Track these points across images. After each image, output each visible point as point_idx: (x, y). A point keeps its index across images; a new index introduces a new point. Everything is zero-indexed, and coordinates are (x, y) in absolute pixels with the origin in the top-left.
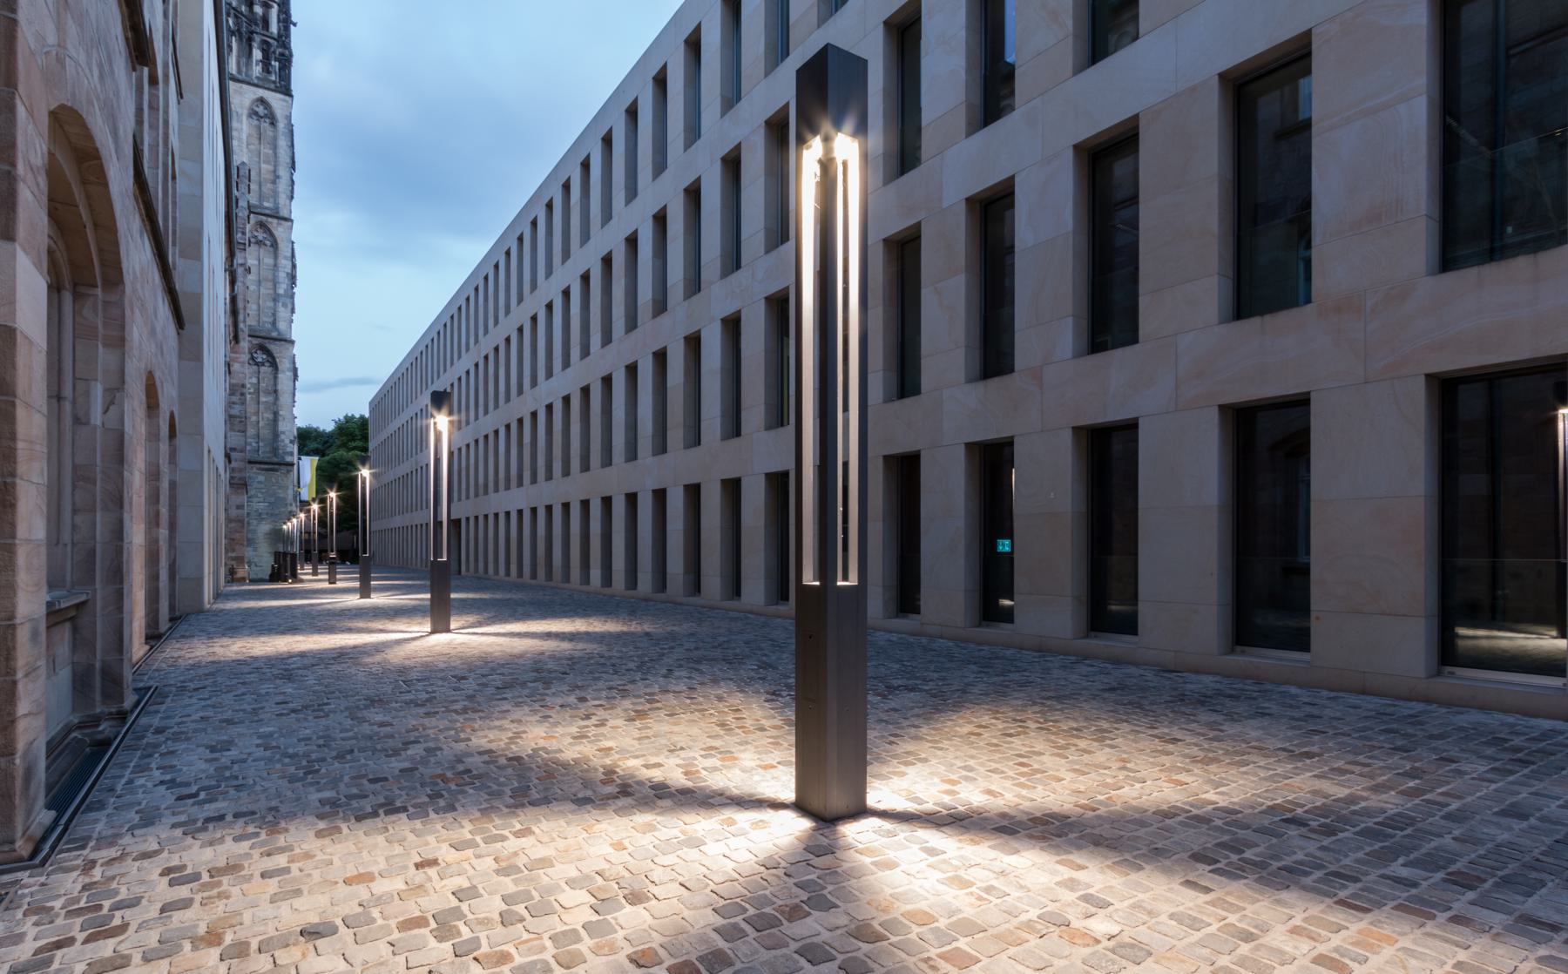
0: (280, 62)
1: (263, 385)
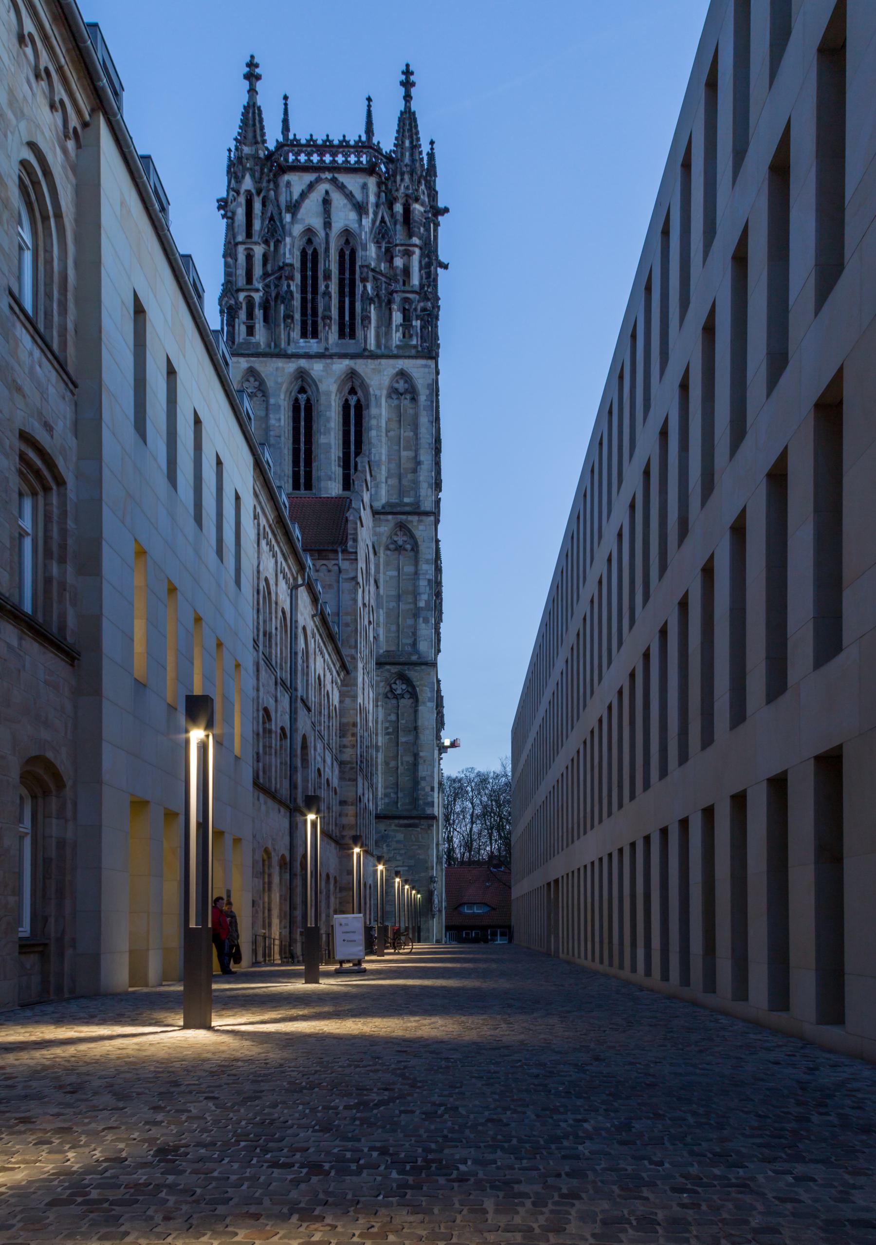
0: (422, 320)
1: (402, 722)
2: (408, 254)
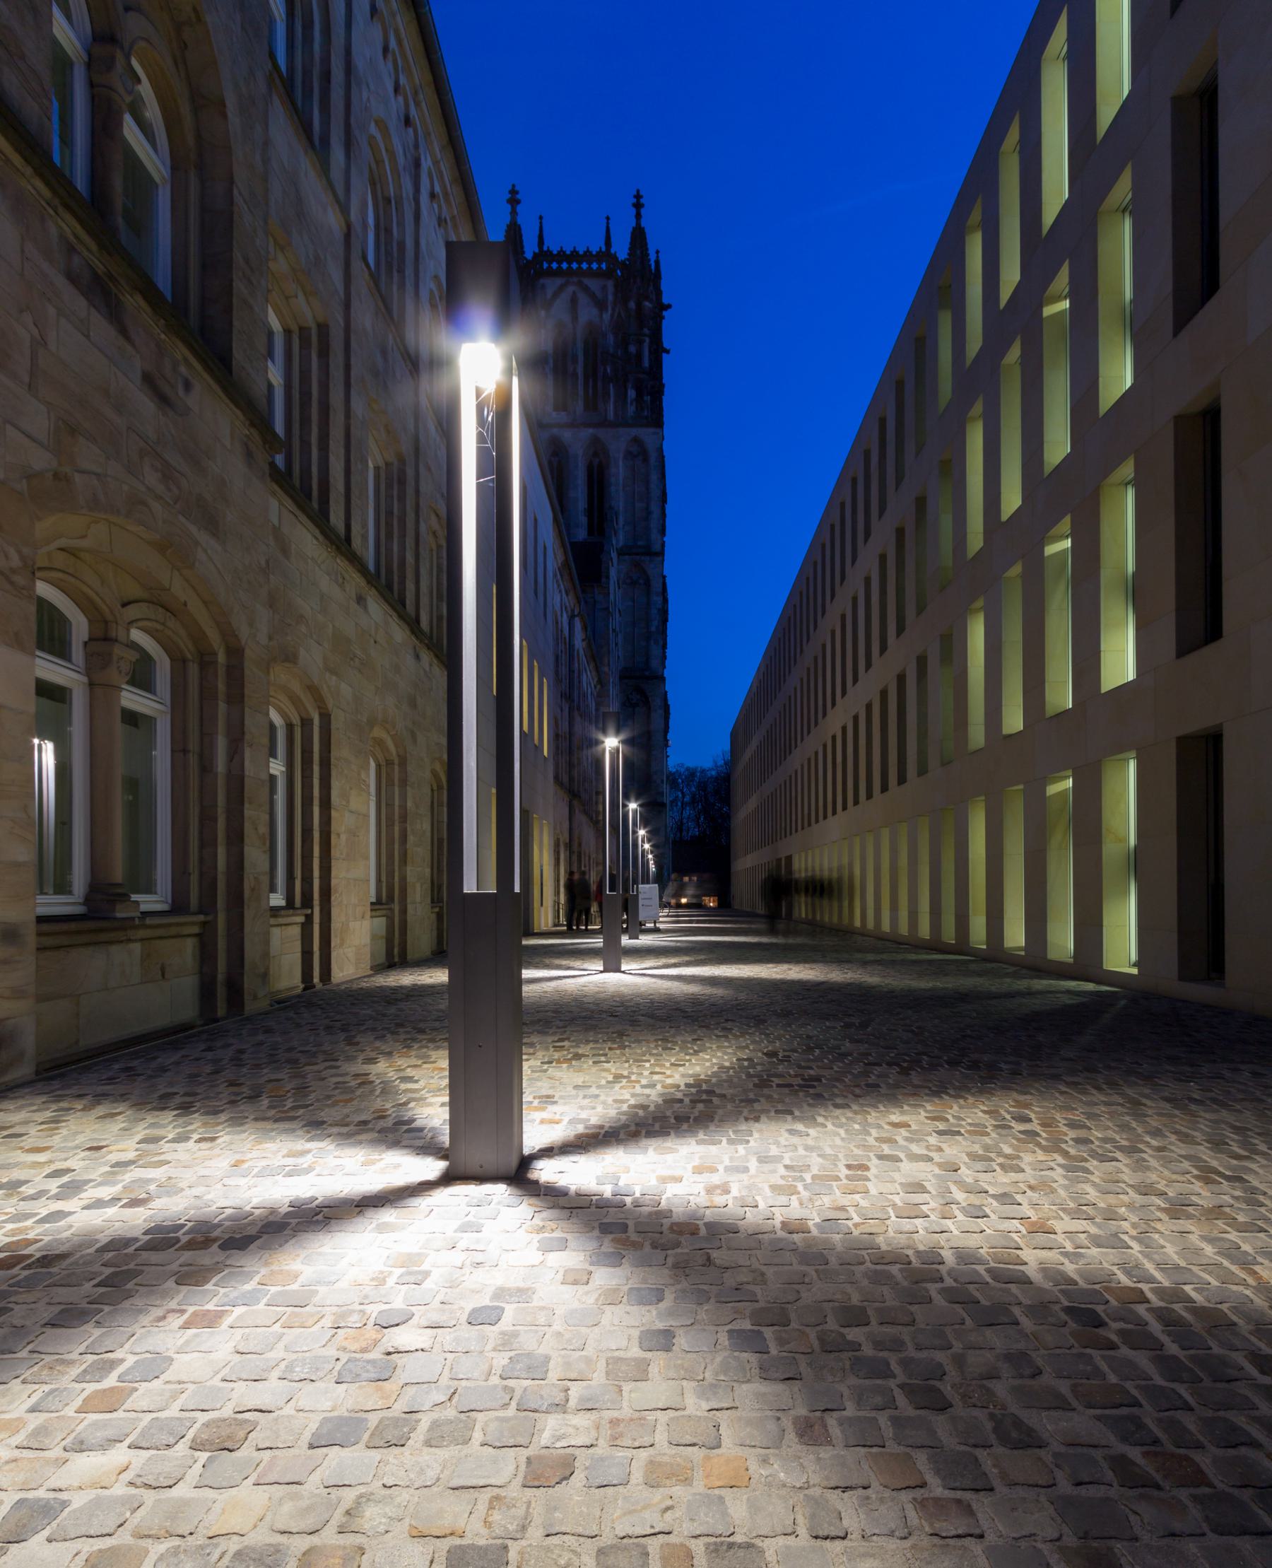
2: (641, 342)
